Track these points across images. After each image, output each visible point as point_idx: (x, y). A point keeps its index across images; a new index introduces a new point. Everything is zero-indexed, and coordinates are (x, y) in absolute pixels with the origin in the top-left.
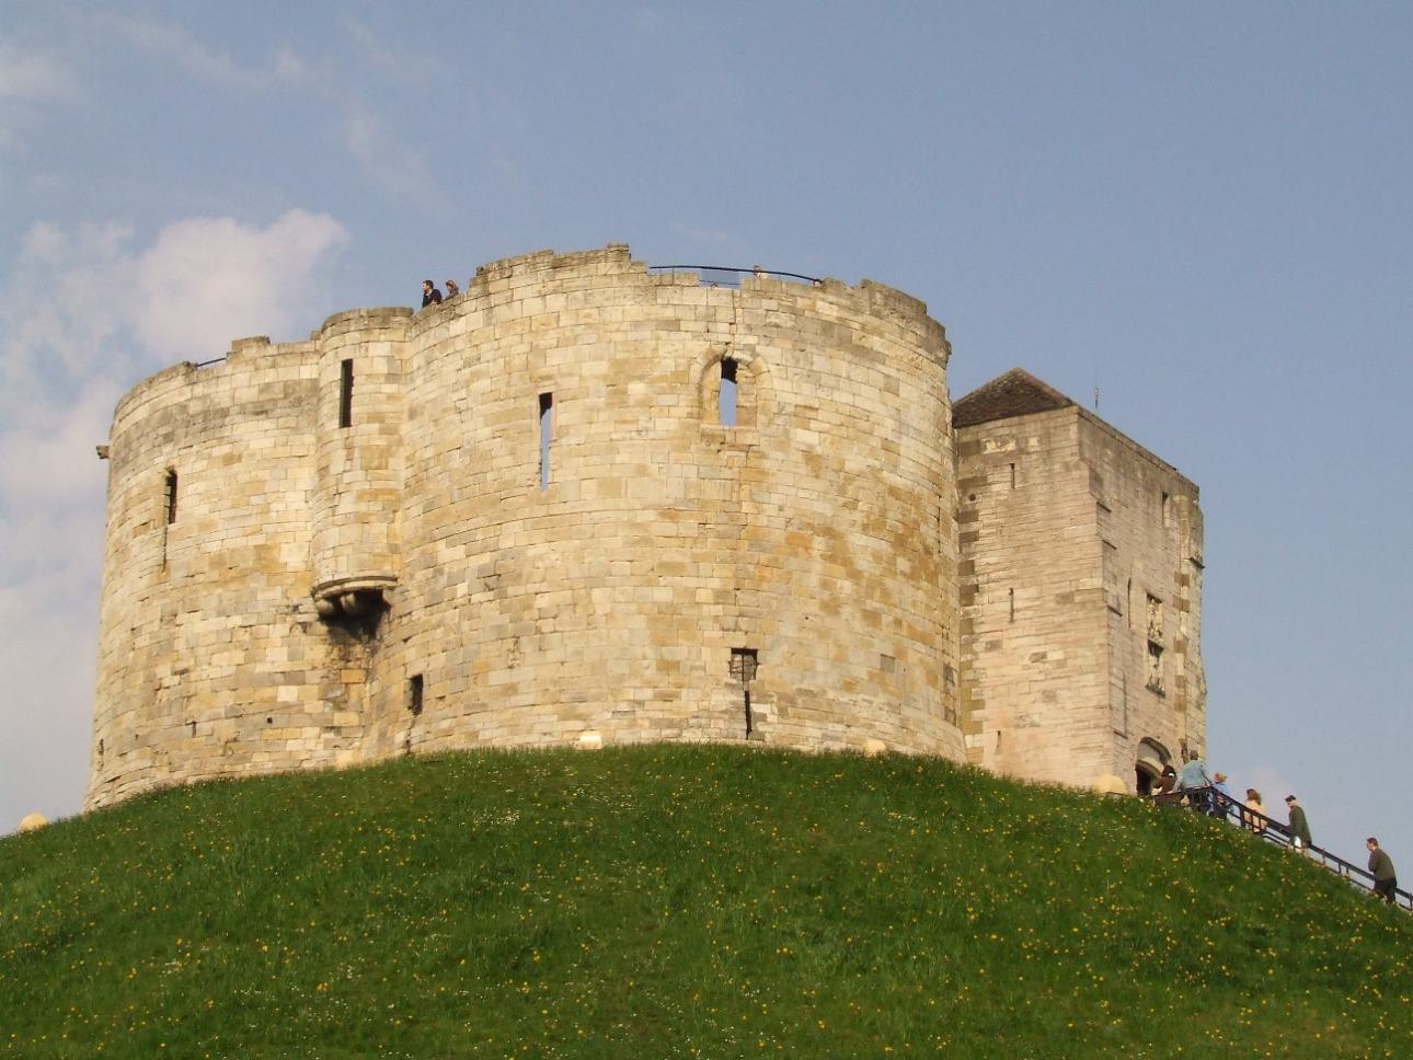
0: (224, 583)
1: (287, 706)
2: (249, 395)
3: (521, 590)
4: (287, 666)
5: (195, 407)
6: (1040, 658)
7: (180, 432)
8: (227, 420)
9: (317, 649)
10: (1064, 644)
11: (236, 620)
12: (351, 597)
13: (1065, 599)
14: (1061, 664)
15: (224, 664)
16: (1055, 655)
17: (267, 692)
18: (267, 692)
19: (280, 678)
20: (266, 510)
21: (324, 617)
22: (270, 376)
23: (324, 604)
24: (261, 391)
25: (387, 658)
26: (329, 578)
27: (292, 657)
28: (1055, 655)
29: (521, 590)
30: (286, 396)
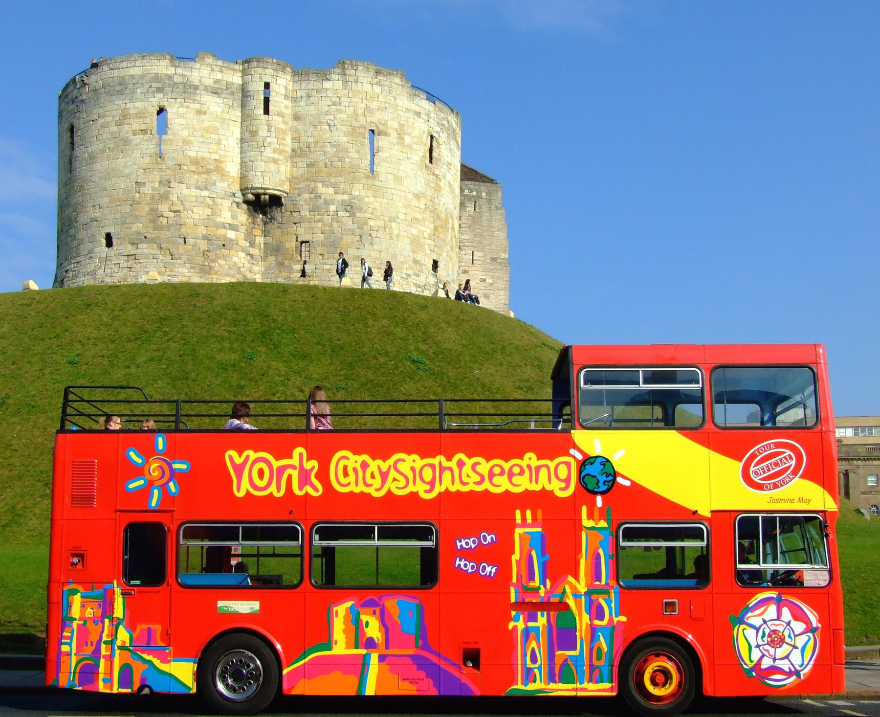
0: (199, 173)
1: (231, 240)
2: (209, 82)
3: (362, 215)
4: (230, 221)
5: (177, 79)
6: (484, 280)
7: (168, 89)
8: (198, 92)
9: (243, 216)
10: (492, 277)
11: (205, 193)
12: (267, 197)
13: (494, 260)
14: (491, 285)
15: (201, 212)
16: (487, 281)
17: (222, 232)
18: (222, 232)
19: (228, 226)
20: (219, 142)
21: (246, 202)
22: (219, 76)
23: (251, 197)
24: (215, 82)
25: (278, 228)
26: (260, 186)
27: (233, 217)
28: (489, 281)
29: (362, 215)
30: (227, 89)
